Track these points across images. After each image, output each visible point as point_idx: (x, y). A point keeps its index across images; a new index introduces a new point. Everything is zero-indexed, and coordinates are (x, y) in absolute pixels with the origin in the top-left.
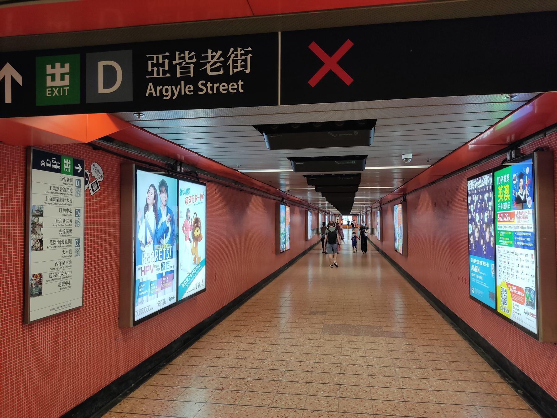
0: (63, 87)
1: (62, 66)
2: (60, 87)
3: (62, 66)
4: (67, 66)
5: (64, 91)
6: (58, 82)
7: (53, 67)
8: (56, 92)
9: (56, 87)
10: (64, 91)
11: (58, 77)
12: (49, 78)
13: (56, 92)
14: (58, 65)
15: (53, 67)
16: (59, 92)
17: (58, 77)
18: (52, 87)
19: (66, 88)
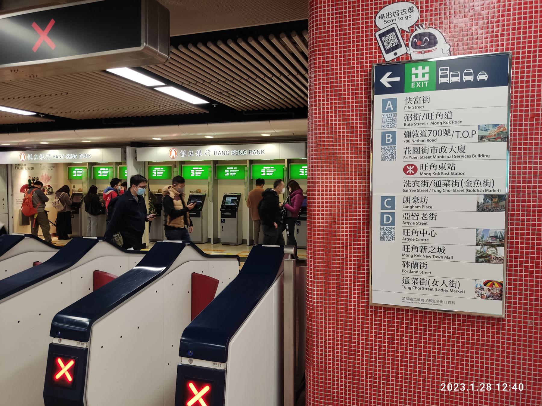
0: (424, 81)
1: (424, 68)
2: (421, 82)
3: (424, 68)
4: (427, 69)
5: (424, 84)
6: (420, 78)
7: (417, 69)
8: (418, 85)
9: (418, 82)
10: (424, 84)
11: (420, 75)
12: (413, 77)
13: (418, 85)
14: (420, 68)
15: (417, 69)
16: (421, 84)
17: (420, 75)
18: (415, 82)
19: (426, 82)
